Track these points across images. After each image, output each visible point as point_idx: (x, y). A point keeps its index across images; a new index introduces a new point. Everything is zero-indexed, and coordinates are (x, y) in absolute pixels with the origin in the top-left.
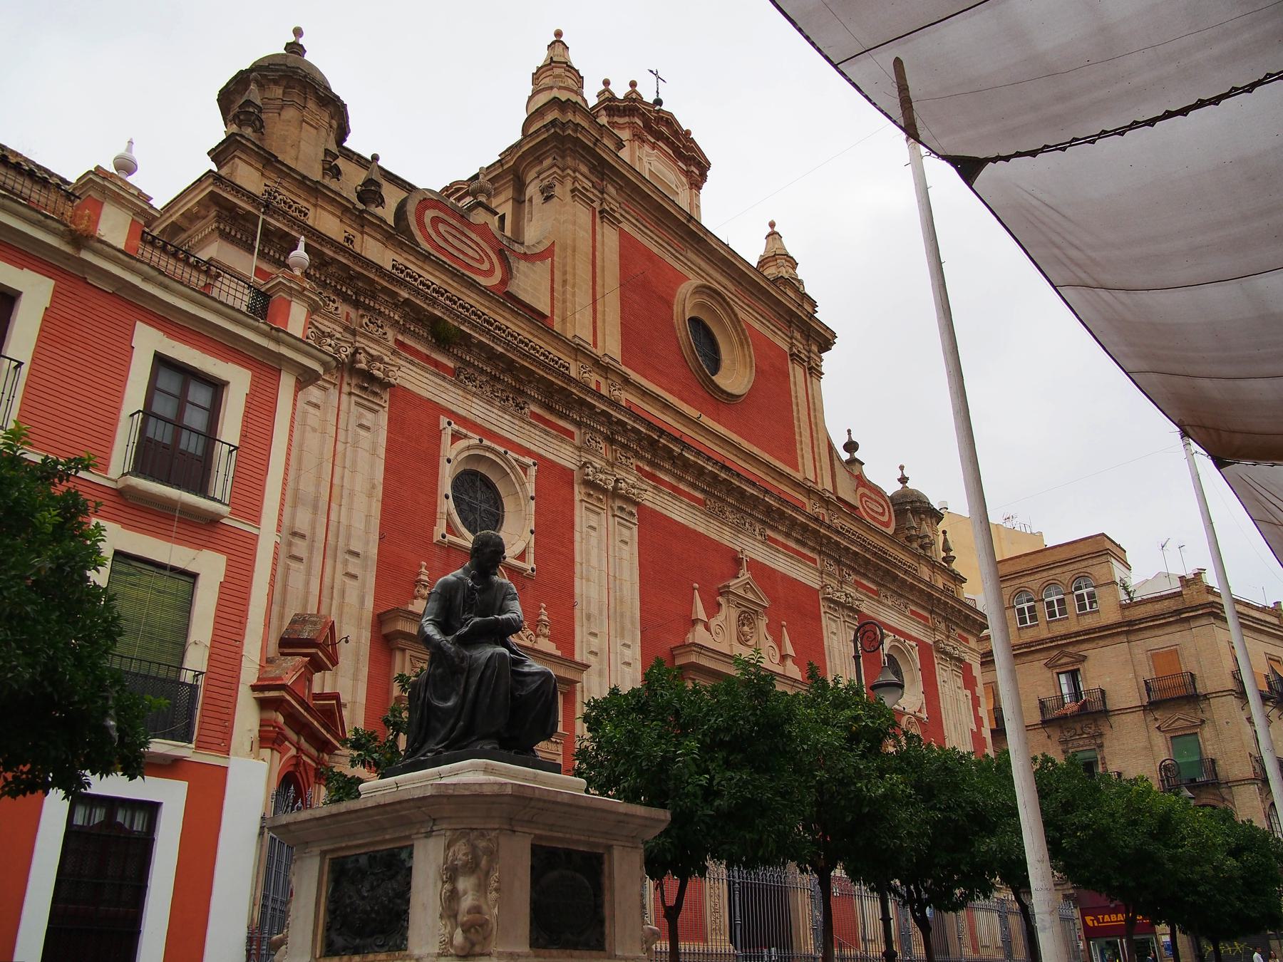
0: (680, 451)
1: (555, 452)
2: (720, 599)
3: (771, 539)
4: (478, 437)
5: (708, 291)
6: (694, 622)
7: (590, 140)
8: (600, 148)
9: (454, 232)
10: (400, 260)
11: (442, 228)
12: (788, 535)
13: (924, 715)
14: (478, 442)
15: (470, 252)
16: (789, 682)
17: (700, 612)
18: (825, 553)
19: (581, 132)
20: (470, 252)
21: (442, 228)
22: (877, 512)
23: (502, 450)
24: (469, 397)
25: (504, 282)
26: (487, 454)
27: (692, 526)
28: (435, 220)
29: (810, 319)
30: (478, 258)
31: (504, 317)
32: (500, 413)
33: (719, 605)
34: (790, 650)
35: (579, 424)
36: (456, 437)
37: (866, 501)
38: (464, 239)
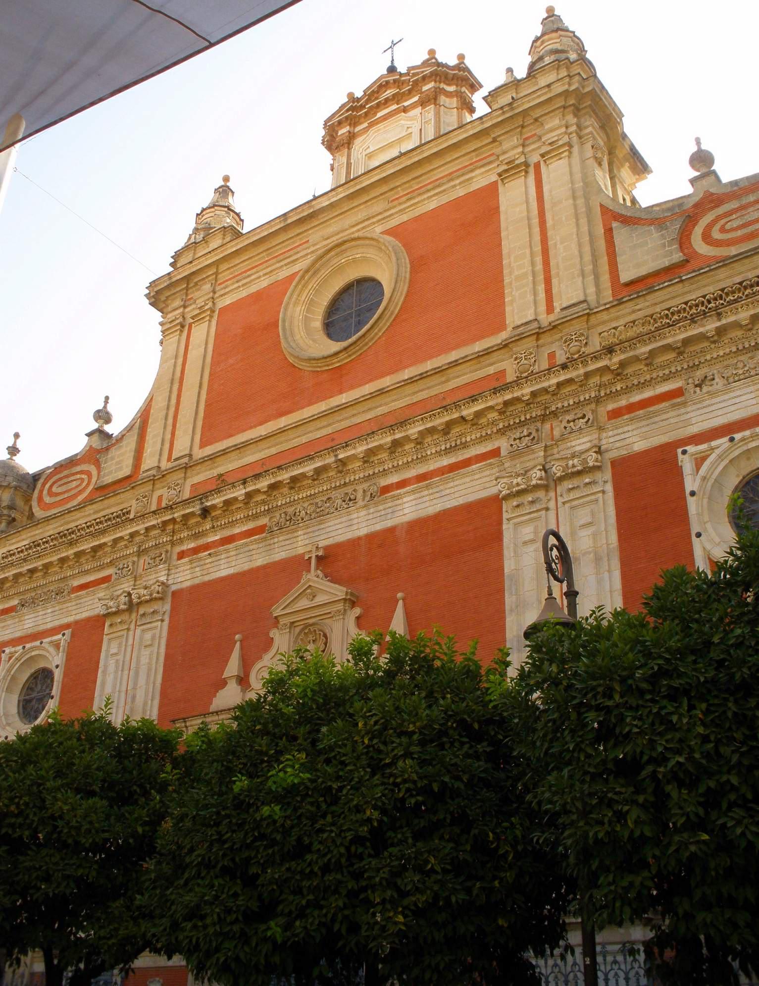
0: (198, 507)
1: (89, 607)
3: (386, 490)
4: (21, 647)
5: (333, 253)
9: (60, 483)
12: (424, 459)
15: (74, 484)
18: (508, 427)
20: (74, 484)
23: (38, 643)
26: (33, 653)
27: (246, 567)
30: (78, 482)
35: (111, 563)
37: (723, 230)
38: (70, 479)
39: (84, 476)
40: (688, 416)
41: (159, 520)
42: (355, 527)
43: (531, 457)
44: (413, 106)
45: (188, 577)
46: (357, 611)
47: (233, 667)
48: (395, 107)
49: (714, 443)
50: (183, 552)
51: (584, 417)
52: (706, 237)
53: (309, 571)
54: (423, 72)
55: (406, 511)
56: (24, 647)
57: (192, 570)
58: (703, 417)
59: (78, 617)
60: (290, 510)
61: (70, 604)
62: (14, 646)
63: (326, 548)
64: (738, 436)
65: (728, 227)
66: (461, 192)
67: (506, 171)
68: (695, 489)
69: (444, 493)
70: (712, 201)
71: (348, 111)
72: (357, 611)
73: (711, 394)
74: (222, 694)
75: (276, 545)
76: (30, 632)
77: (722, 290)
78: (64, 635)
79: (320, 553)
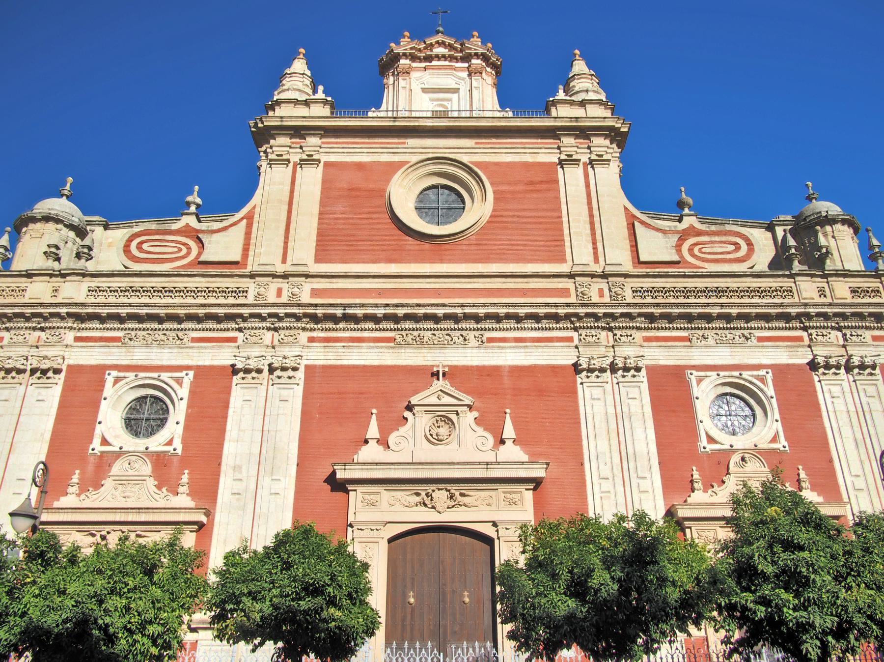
2: (407, 414)
3: (490, 340)
6: (366, 442)
7: (277, 121)
8: (287, 121)
10: (93, 285)
11: (145, 246)
13: (782, 444)
14: (134, 377)
16: (483, 466)
17: (373, 431)
19: (266, 121)
21: (145, 246)
22: (729, 253)
24: (131, 350)
25: (199, 255)
28: (139, 247)
29: (577, 122)
30: (176, 250)
31: (182, 282)
32: (159, 351)
33: (406, 419)
34: (509, 432)
35: (240, 330)
36: (117, 380)
37: (700, 251)
39: (183, 247)
40: (692, 354)
41: (301, 311)
42: (469, 358)
43: (596, 349)
44: (461, 69)
45: (322, 358)
46: (475, 414)
47: (373, 431)
48: (447, 63)
49: (709, 373)
50: (313, 337)
51: (631, 336)
52: (691, 251)
53: (438, 379)
54: (475, 49)
55: (508, 358)
56: (136, 376)
57: (326, 354)
58: (699, 357)
59: (201, 363)
60: (416, 333)
61: (191, 351)
62: (119, 371)
63: (450, 367)
64: (722, 373)
65: (704, 250)
66: (529, 159)
67: (565, 160)
68: (699, 396)
69: (534, 354)
70: (694, 232)
71: (411, 49)
72: (475, 414)
73: (706, 347)
74: (365, 449)
75: (403, 354)
76: (140, 363)
77: (706, 288)
78: (187, 374)
79: (446, 369)
